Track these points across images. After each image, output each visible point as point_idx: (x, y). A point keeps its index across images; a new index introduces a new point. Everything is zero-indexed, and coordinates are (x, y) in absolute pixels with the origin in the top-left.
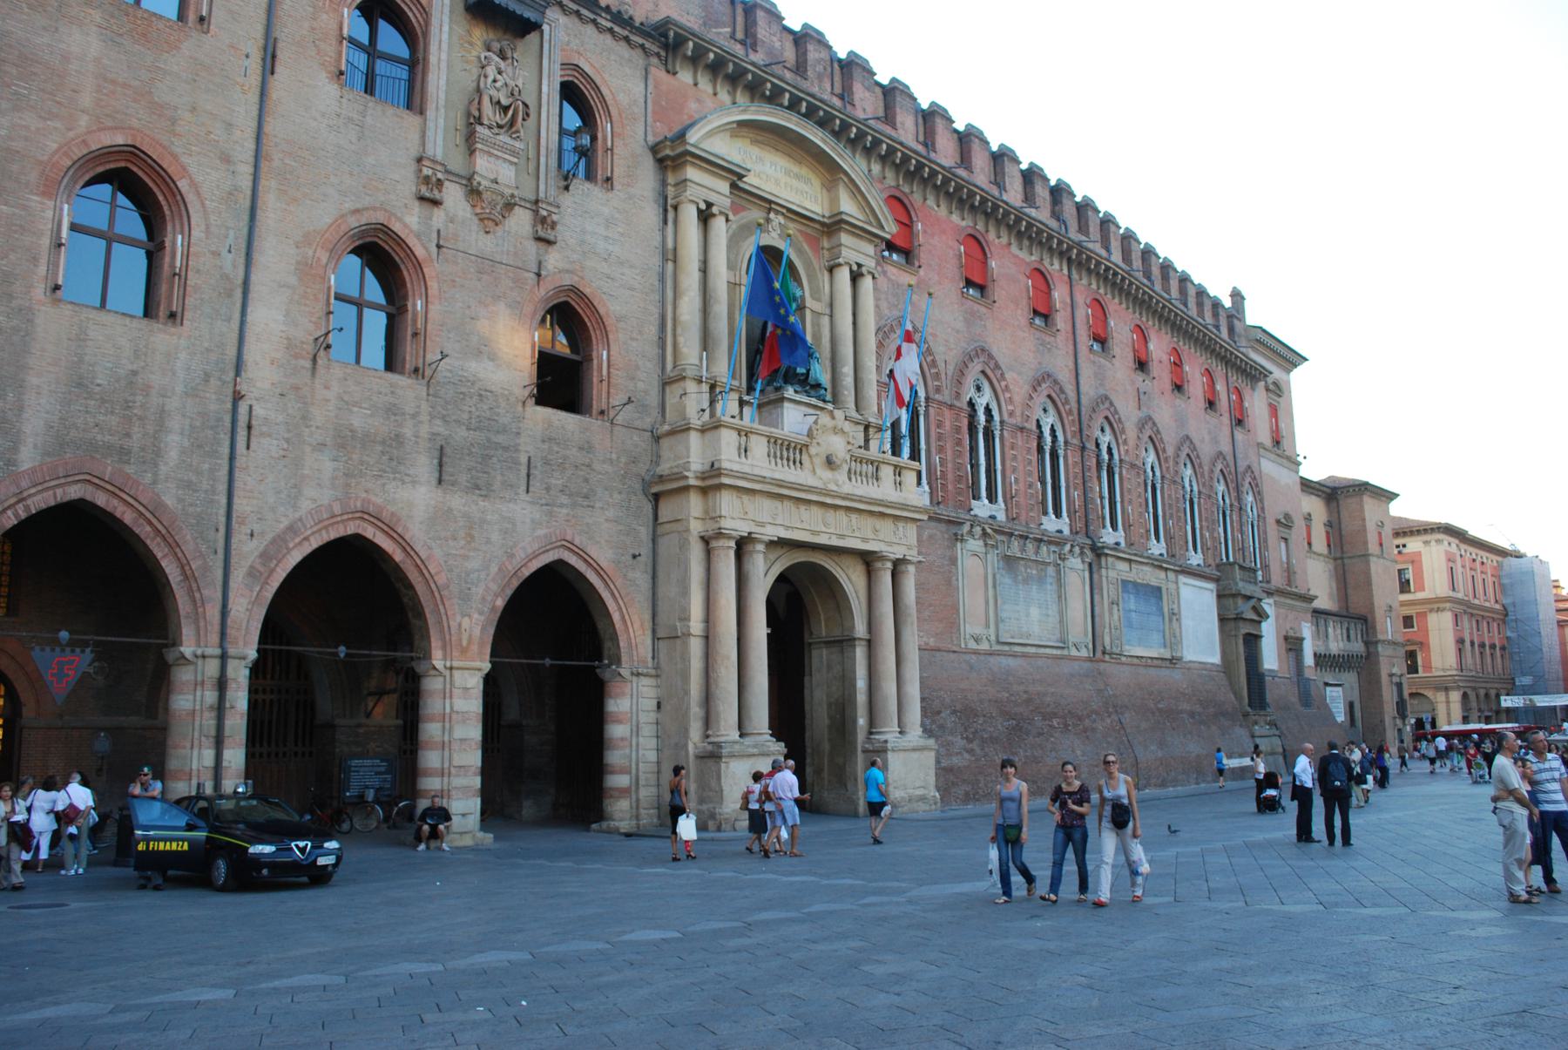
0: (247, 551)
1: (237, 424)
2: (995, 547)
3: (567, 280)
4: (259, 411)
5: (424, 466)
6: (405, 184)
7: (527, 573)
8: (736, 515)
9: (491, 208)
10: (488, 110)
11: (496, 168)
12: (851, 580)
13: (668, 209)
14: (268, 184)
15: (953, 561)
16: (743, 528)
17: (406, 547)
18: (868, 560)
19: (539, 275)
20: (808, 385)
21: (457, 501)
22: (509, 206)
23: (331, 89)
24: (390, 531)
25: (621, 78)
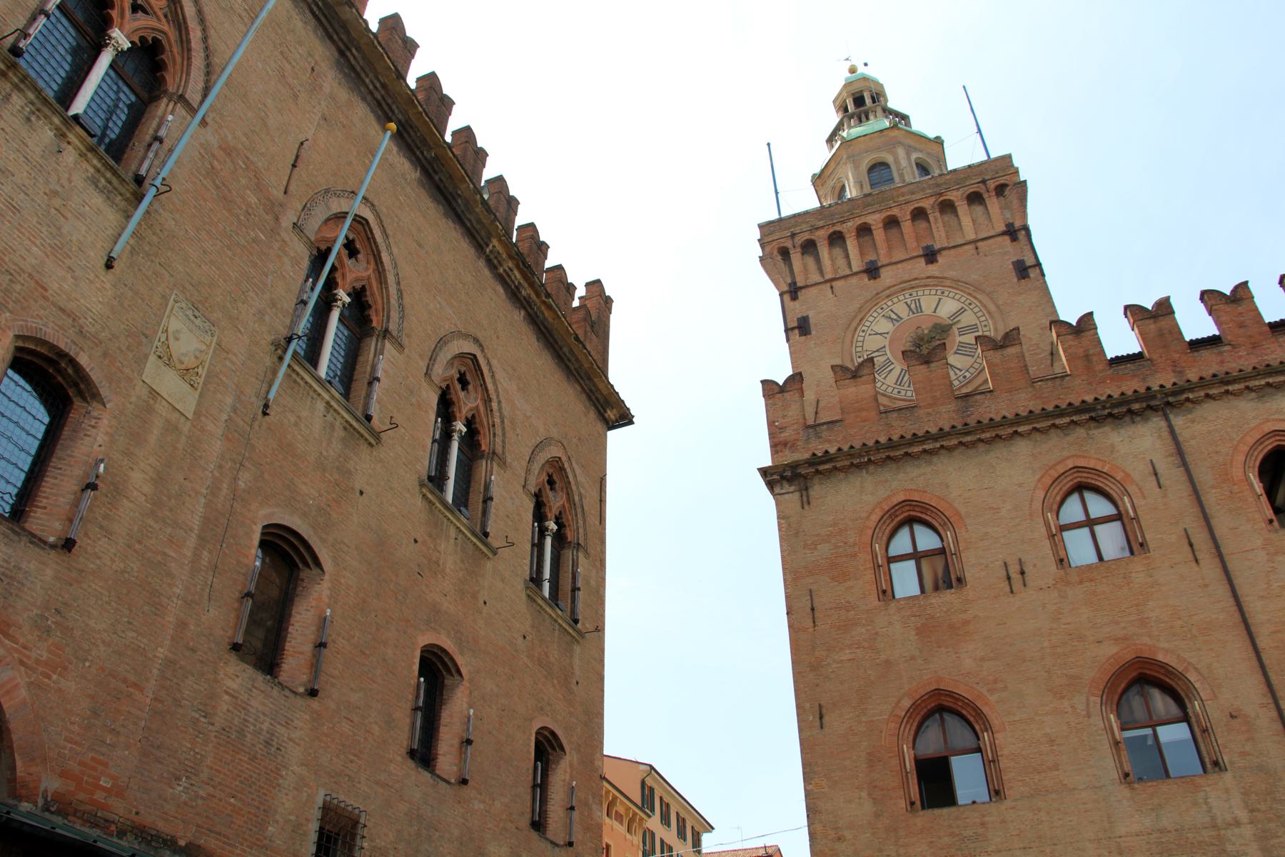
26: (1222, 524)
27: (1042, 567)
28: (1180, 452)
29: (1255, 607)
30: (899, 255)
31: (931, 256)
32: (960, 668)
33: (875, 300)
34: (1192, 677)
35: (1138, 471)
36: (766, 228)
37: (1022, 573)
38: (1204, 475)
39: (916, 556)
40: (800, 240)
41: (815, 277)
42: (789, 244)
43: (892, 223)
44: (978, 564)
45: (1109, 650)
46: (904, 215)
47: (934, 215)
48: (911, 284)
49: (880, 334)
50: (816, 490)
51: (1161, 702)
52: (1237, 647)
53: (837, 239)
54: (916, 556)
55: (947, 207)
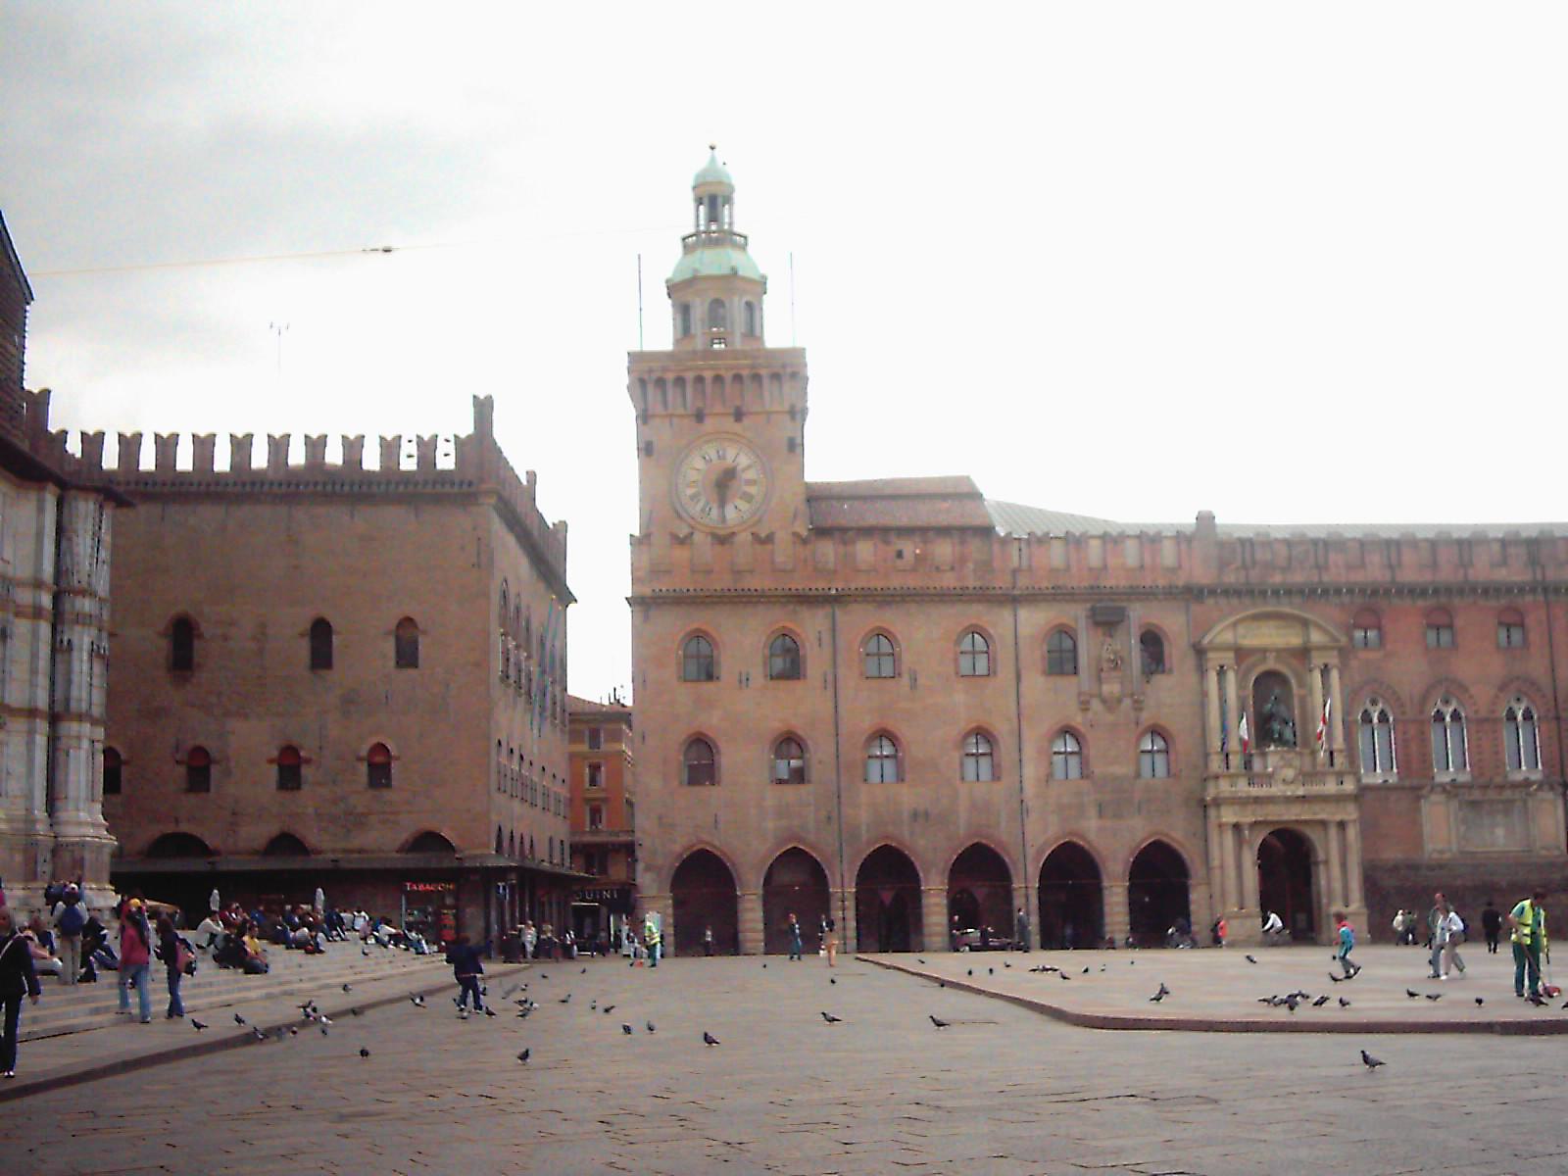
0: (1031, 852)
1: (1023, 809)
2: (1456, 795)
3: (1152, 722)
4: (1030, 804)
5: (1092, 812)
7: (1142, 847)
8: (1229, 816)
9: (1110, 704)
10: (1105, 666)
12: (1314, 835)
14: (1024, 724)
15: (1418, 810)
16: (1233, 820)
17: (1089, 842)
18: (1324, 824)
19: (1137, 723)
20: (1281, 741)
22: (1120, 701)
24: (1084, 839)
25: (1173, 622)
26: (842, 672)
28: (834, 630)
31: (739, 415)
32: (712, 722)
34: (809, 742)
36: (637, 359)
37: (747, 679)
38: (841, 643)
40: (654, 376)
41: (660, 410)
42: (646, 377)
43: (718, 379)
46: (728, 375)
47: (747, 382)
49: (698, 467)
51: (794, 749)
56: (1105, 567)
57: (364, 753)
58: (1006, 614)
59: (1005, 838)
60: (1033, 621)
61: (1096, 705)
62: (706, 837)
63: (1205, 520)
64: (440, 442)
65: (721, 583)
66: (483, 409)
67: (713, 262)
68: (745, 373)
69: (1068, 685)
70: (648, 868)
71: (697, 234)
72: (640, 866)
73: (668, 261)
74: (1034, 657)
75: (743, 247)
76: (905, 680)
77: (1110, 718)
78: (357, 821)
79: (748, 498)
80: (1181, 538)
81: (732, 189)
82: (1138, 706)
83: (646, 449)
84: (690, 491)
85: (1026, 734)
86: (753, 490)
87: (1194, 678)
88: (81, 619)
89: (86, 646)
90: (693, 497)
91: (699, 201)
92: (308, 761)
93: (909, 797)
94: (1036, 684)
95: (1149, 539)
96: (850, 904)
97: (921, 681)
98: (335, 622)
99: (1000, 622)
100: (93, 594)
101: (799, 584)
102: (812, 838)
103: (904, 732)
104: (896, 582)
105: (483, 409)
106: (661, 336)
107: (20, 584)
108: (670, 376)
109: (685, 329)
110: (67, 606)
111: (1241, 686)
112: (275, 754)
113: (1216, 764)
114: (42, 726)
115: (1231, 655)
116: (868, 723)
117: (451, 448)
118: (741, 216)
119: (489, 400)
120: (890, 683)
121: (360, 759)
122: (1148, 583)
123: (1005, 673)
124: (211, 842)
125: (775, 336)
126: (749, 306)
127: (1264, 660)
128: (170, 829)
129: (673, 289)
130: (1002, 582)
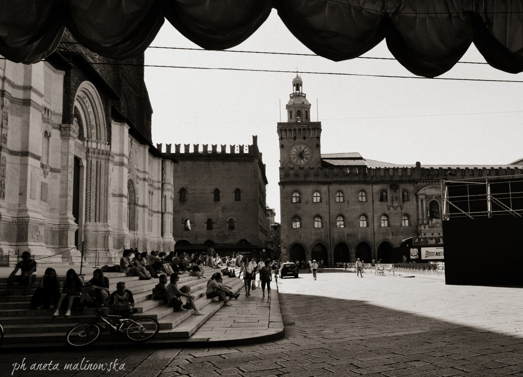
0: (376, 244)
1: (374, 234)
5: (391, 234)
6: (386, 208)
9: (395, 208)
11: (396, 204)
13: (417, 201)
21: (394, 237)
22: (397, 207)
23: (378, 202)
27: (310, 203)
29: (331, 210)
30: (300, 137)
31: (304, 138)
32: (299, 212)
33: (294, 145)
35: (323, 192)
36: (279, 124)
38: (331, 194)
39: (296, 197)
41: (285, 137)
43: (299, 129)
44: (303, 201)
45: (315, 213)
48: (301, 144)
50: (285, 186)
52: (328, 214)
53: (290, 130)
54: (296, 197)
55: (309, 129)
56: (394, 175)
57: (228, 221)
58: (370, 186)
59: (369, 240)
60: (377, 188)
61: (392, 208)
62: (298, 240)
63: (418, 164)
64: (245, 147)
65: (302, 178)
66: (255, 138)
67: (299, 101)
68: (306, 128)
69: (385, 204)
70: (284, 248)
71: (294, 93)
72: (282, 247)
73: (287, 100)
74: (377, 198)
75: (305, 97)
76: (346, 203)
77: (396, 212)
78: (227, 237)
79: (307, 158)
80: (412, 169)
81: (302, 82)
82: (402, 209)
83: (282, 146)
84: (293, 157)
85: (375, 216)
86: (308, 156)
87: (415, 202)
88: (168, 190)
89: (170, 197)
90: (294, 158)
91: (294, 85)
92: (214, 223)
93: (347, 231)
94: (377, 203)
95: (405, 170)
96: (333, 256)
97: (350, 203)
98: (221, 190)
99: (368, 188)
100: (171, 184)
101: (320, 179)
102: (323, 240)
103: (346, 215)
104: (343, 179)
105: (255, 138)
106: (285, 119)
107: (155, 182)
108: (288, 128)
109: (291, 117)
110: (165, 187)
111: (426, 204)
112: (206, 221)
113: (420, 222)
114: (160, 215)
115: (424, 196)
116: (337, 212)
117: (247, 148)
118: (304, 89)
119: (256, 136)
120: (342, 204)
121: (227, 222)
122: (404, 179)
123: (370, 200)
124: (191, 242)
125: (313, 119)
126: (306, 111)
127: (432, 198)
128: (181, 239)
129: (288, 107)
130: (369, 179)
